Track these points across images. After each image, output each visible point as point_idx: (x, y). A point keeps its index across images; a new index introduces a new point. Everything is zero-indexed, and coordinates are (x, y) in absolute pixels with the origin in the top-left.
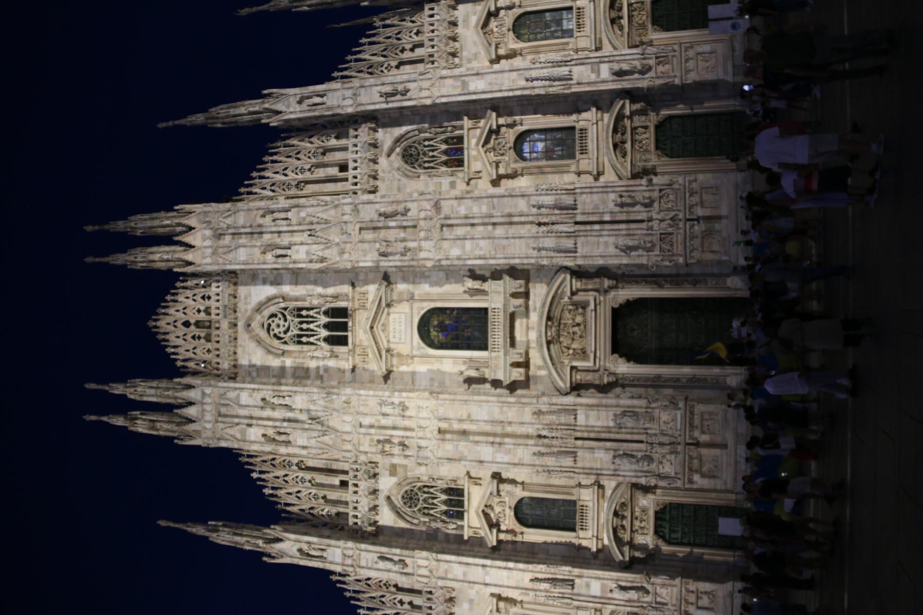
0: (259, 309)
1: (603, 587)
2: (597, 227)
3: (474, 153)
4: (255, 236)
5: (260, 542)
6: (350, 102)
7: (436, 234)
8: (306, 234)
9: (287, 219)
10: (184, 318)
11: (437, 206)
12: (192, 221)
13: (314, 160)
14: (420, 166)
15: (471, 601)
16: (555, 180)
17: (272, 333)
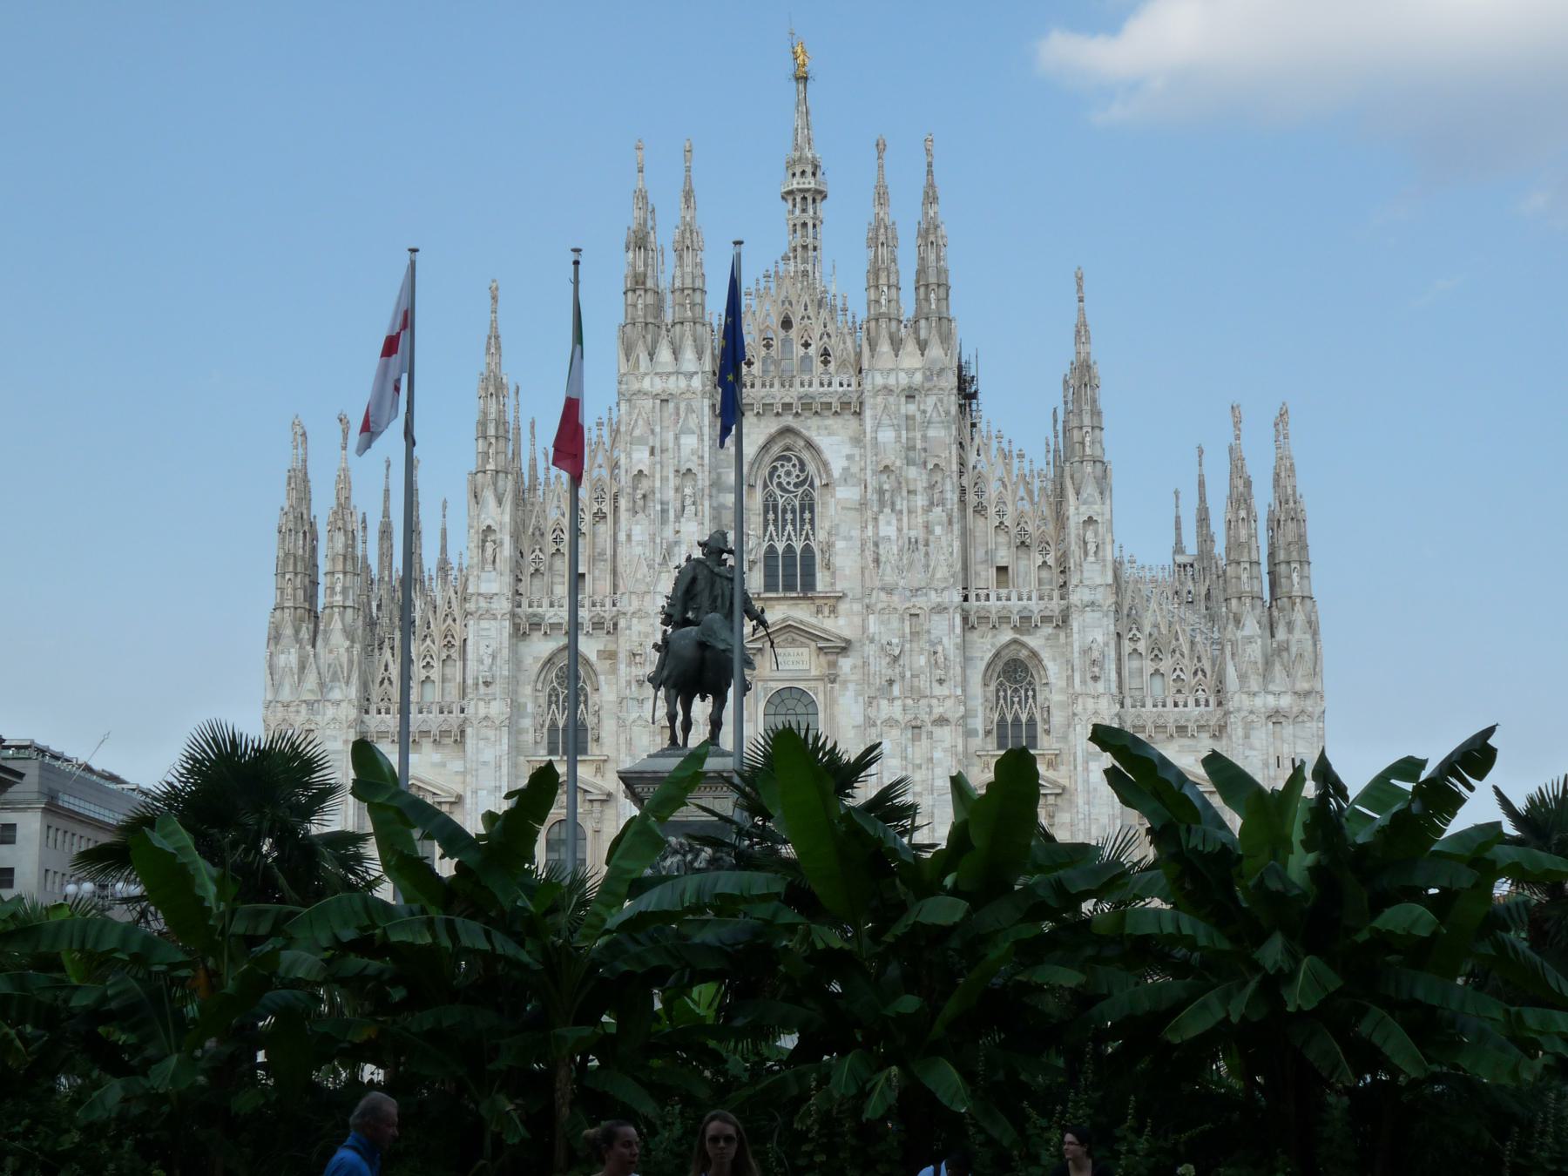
0: (809, 445)
4: (911, 454)
5: (491, 466)
9: (932, 504)
10: (795, 321)
11: (942, 721)
12: (935, 351)
14: (1001, 684)
15: (443, 765)
17: (778, 464)
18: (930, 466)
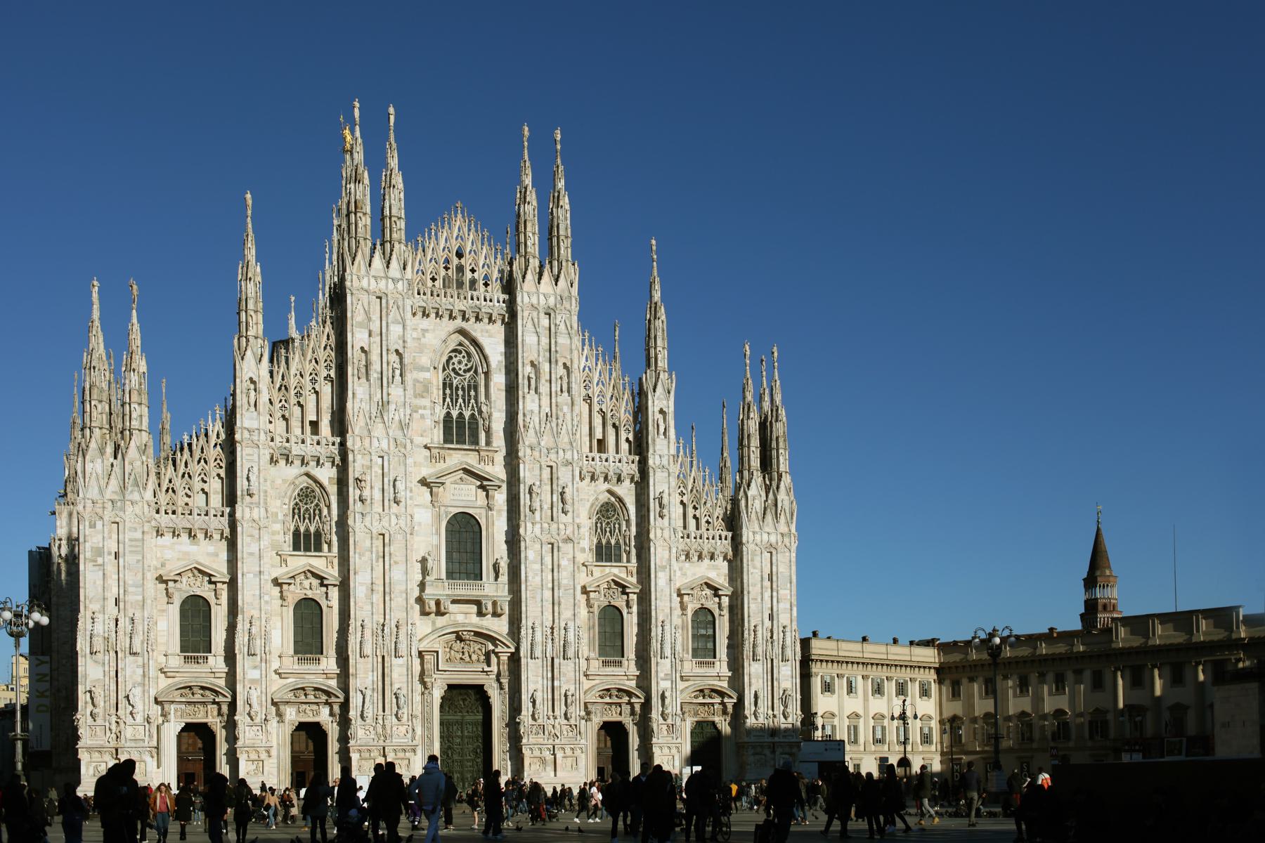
0: (474, 342)
1: (253, 681)
2: (550, 675)
3: (607, 570)
6: (658, 462)
7: (545, 538)
8: (548, 410)
11: (569, 540)
13: (609, 415)
16: (584, 641)
18: (560, 364)
